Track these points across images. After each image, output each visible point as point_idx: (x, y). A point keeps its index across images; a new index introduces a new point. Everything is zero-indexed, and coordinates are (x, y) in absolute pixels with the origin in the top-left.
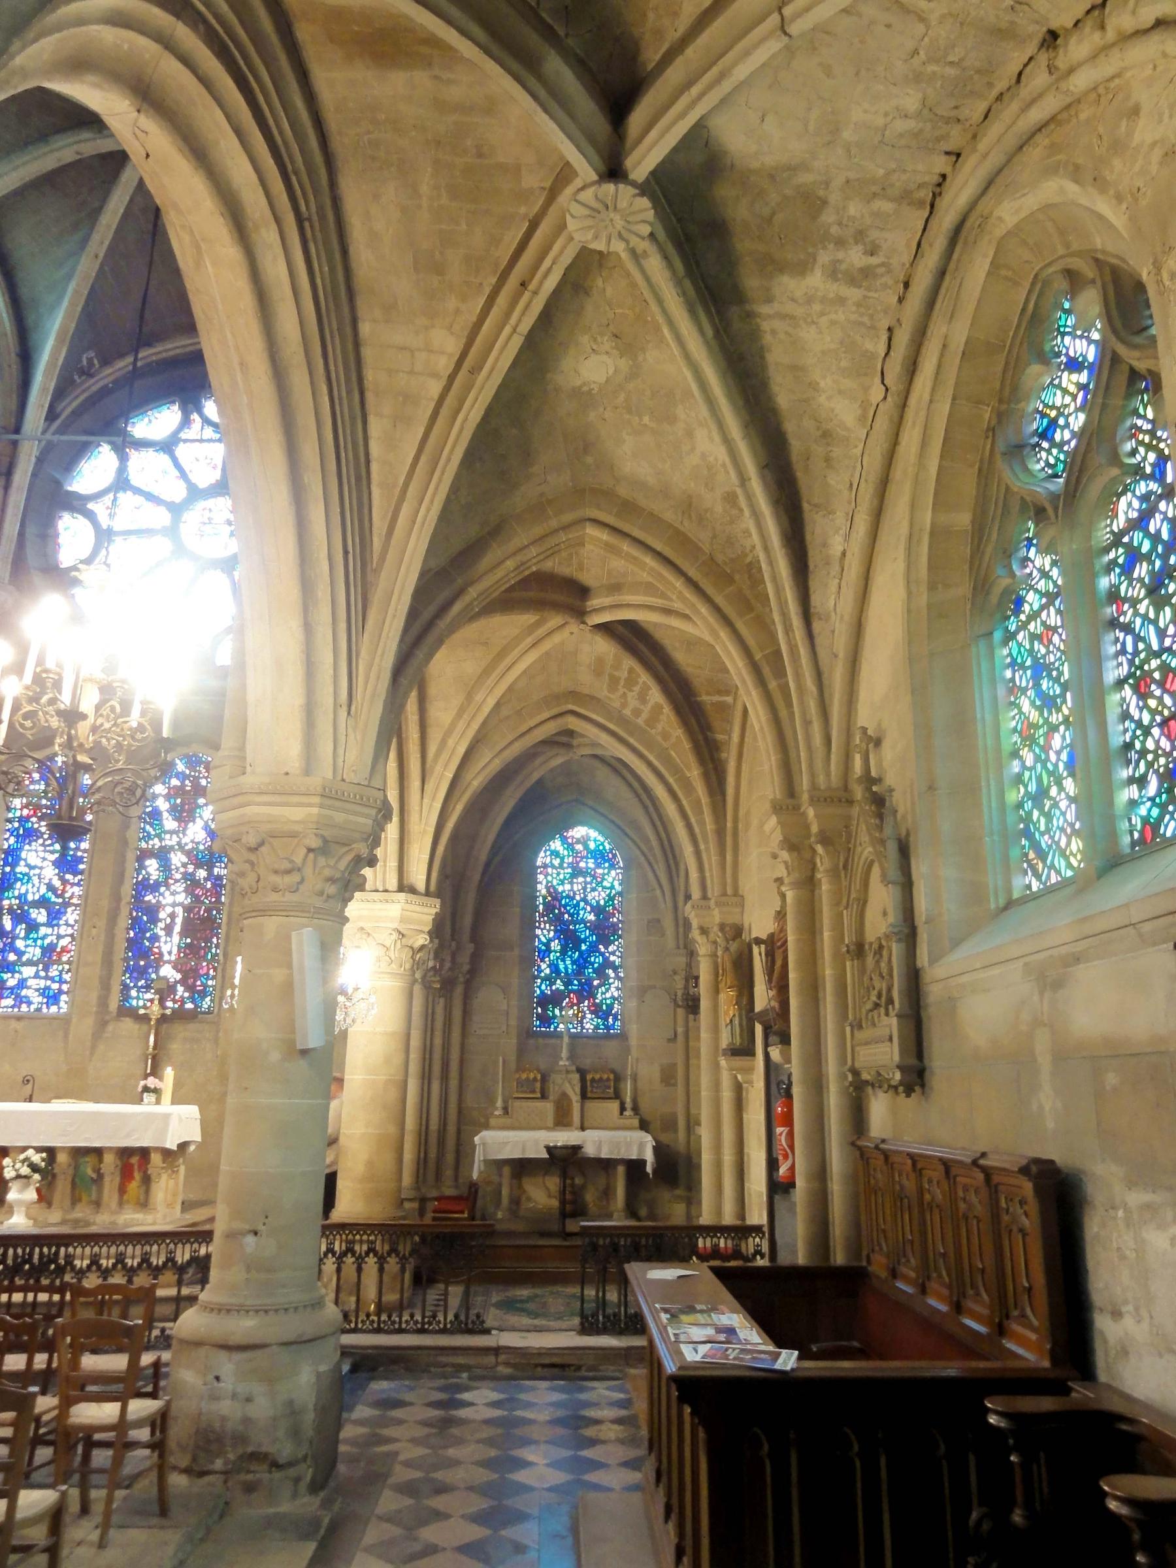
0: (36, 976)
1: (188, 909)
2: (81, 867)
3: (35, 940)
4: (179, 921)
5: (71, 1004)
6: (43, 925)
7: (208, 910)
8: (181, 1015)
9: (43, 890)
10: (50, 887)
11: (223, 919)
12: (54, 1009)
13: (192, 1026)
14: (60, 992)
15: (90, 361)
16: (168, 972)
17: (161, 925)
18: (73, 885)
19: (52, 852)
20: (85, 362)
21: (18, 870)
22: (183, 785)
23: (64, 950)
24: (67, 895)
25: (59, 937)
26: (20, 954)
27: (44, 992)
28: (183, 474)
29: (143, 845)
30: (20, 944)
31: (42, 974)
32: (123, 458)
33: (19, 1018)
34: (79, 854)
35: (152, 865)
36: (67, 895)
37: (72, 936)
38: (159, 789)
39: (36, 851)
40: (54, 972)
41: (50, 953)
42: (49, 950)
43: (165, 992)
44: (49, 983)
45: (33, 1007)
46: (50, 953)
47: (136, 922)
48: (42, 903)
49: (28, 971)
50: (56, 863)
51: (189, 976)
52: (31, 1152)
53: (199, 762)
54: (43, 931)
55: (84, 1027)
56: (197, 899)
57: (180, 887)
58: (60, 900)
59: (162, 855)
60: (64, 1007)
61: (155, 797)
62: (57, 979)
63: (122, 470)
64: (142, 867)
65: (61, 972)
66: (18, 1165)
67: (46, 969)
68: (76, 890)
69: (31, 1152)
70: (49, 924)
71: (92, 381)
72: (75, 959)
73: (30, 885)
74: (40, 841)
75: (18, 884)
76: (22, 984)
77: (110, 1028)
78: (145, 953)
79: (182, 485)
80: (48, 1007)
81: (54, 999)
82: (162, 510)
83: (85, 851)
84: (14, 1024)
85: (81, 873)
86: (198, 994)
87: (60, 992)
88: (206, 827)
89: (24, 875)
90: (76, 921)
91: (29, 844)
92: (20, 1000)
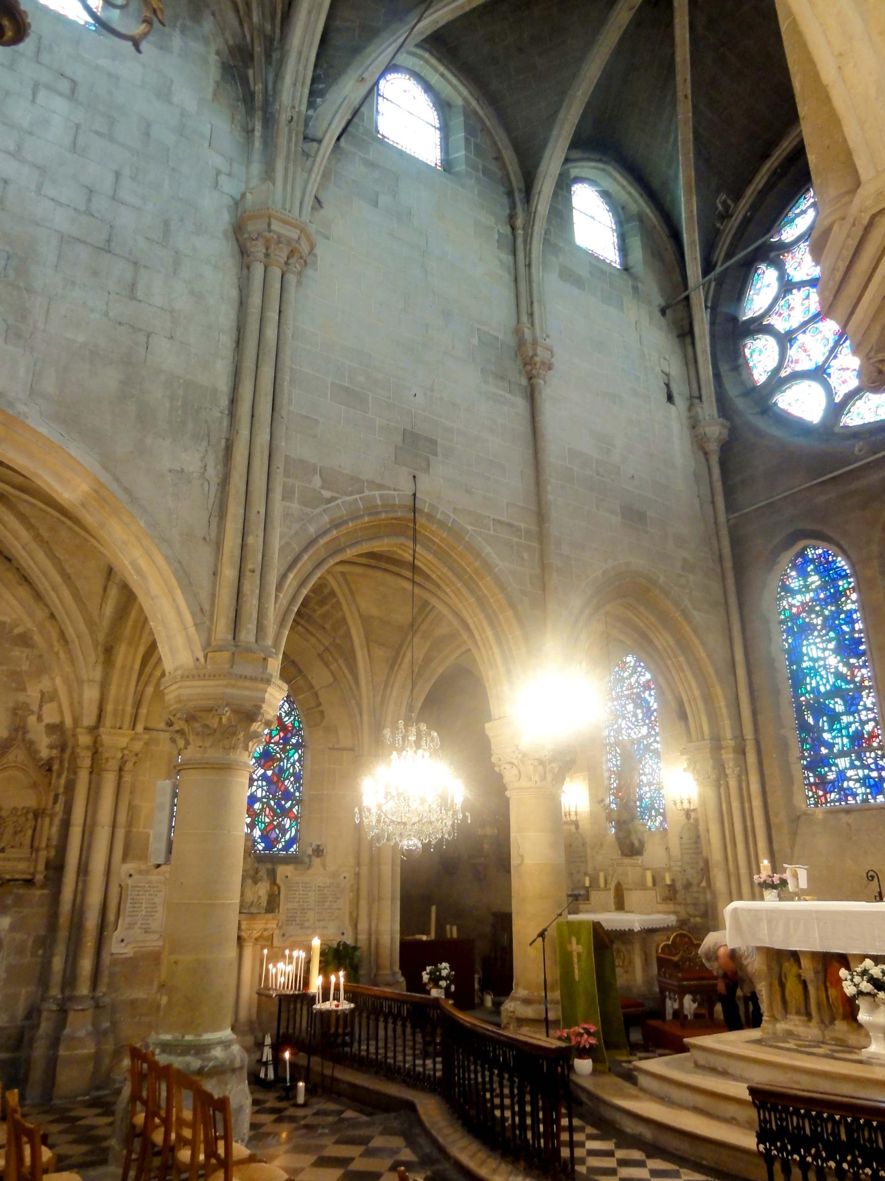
0: (853, 767)
2: (862, 647)
3: (840, 731)
6: (843, 714)
9: (832, 679)
10: (838, 675)
15: (724, 203)
18: (860, 668)
19: (830, 641)
20: (720, 207)
21: (804, 665)
23: (872, 736)
24: (857, 679)
25: (863, 723)
26: (830, 746)
27: (864, 781)
30: (826, 736)
31: (857, 763)
33: (848, 811)
34: (856, 635)
36: (857, 679)
37: (874, 719)
39: (815, 644)
41: (857, 738)
42: (857, 738)
44: (866, 772)
45: (859, 798)
48: (836, 692)
49: (843, 763)
50: (837, 651)
52: (868, 963)
54: (845, 719)
58: (852, 686)
62: (873, 766)
65: (875, 759)
66: (857, 979)
67: (859, 758)
68: (864, 671)
69: (868, 963)
70: (848, 712)
71: (734, 218)
73: (818, 678)
74: (816, 633)
75: (808, 680)
76: (842, 776)
80: (875, 798)
83: (860, 631)
84: (844, 818)
85: (863, 653)
89: (811, 668)
90: (873, 703)
91: (808, 640)
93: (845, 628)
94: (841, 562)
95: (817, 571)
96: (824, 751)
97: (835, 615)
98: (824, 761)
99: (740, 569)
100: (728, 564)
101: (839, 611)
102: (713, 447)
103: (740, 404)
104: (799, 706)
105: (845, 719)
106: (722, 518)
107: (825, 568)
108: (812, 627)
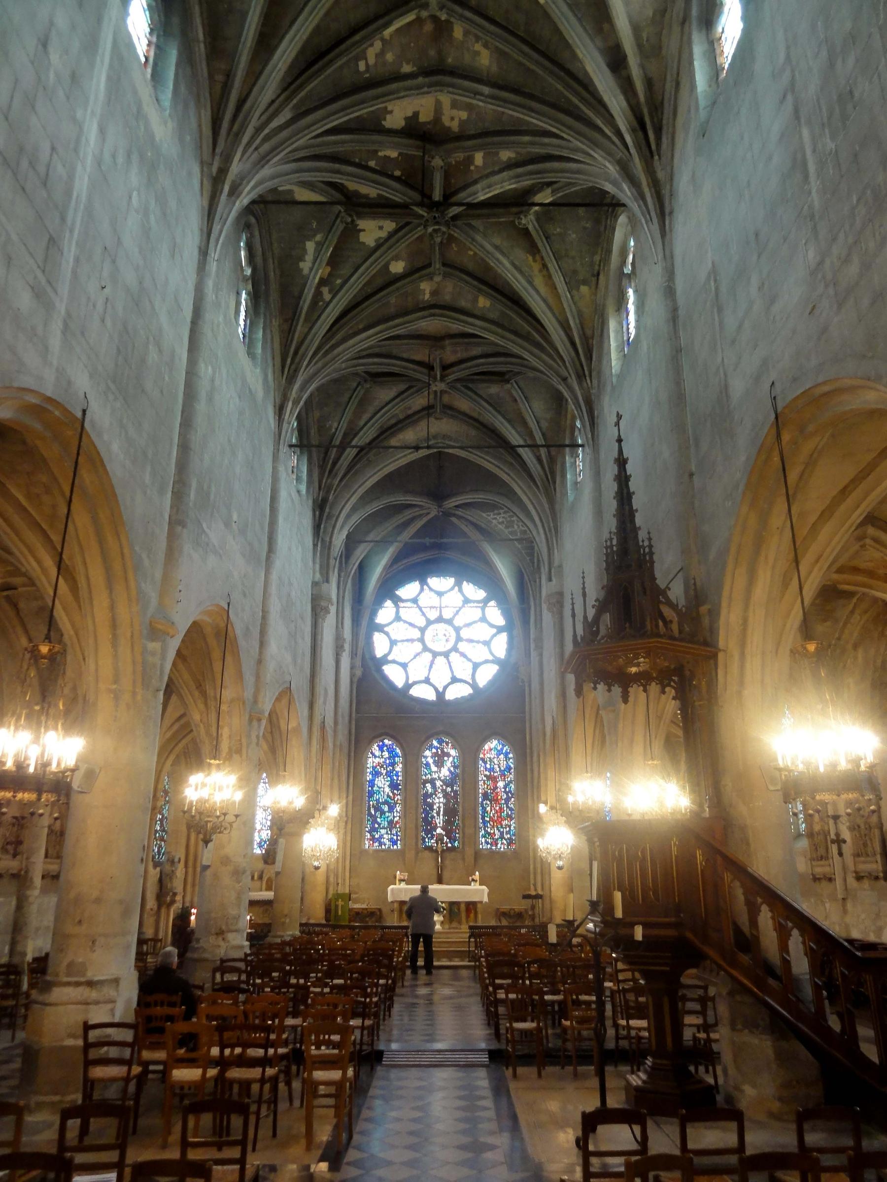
0: (387, 833)
1: (444, 804)
4: (442, 809)
5: (404, 845)
7: (454, 805)
10: (388, 796)
11: (460, 809)
12: (395, 847)
13: (453, 854)
14: (397, 840)
16: (439, 831)
23: (397, 822)
25: (394, 817)
26: (379, 824)
27: (391, 840)
28: (424, 614)
30: (379, 820)
32: (397, 607)
33: (383, 851)
35: (429, 786)
38: (428, 753)
40: (394, 832)
41: (391, 823)
42: (391, 823)
43: (440, 839)
46: (391, 824)
47: (425, 810)
48: (386, 803)
49: (383, 831)
50: (389, 786)
53: (443, 741)
54: (387, 814)
55: (410, 855)
56: (448, 801)
57: (441, 795)
59: (432, 782)
60: (399, 847)
61: (426, 757)
63: (397, 612)
64: (425, 787)
76: (381, 837)
78: (430, 823)
79: (423, 619)
81: (394, 843)
82: (417, 630)
84: (383, 854)
86: (452, 839)
87: (397, 840)
88: (449, 770)
92: (381, 844)
93: (395, 778)
94: (398, 751)
95: (388, 750)
96: (376, 826)
97: (391, 771)
98: (376, 830)
100: (353, 738)
101: (394, 770)
102: (355, 680)
104: (369, 805)
105: (387, 814)
106: (354, 715)
107: (391, 750)
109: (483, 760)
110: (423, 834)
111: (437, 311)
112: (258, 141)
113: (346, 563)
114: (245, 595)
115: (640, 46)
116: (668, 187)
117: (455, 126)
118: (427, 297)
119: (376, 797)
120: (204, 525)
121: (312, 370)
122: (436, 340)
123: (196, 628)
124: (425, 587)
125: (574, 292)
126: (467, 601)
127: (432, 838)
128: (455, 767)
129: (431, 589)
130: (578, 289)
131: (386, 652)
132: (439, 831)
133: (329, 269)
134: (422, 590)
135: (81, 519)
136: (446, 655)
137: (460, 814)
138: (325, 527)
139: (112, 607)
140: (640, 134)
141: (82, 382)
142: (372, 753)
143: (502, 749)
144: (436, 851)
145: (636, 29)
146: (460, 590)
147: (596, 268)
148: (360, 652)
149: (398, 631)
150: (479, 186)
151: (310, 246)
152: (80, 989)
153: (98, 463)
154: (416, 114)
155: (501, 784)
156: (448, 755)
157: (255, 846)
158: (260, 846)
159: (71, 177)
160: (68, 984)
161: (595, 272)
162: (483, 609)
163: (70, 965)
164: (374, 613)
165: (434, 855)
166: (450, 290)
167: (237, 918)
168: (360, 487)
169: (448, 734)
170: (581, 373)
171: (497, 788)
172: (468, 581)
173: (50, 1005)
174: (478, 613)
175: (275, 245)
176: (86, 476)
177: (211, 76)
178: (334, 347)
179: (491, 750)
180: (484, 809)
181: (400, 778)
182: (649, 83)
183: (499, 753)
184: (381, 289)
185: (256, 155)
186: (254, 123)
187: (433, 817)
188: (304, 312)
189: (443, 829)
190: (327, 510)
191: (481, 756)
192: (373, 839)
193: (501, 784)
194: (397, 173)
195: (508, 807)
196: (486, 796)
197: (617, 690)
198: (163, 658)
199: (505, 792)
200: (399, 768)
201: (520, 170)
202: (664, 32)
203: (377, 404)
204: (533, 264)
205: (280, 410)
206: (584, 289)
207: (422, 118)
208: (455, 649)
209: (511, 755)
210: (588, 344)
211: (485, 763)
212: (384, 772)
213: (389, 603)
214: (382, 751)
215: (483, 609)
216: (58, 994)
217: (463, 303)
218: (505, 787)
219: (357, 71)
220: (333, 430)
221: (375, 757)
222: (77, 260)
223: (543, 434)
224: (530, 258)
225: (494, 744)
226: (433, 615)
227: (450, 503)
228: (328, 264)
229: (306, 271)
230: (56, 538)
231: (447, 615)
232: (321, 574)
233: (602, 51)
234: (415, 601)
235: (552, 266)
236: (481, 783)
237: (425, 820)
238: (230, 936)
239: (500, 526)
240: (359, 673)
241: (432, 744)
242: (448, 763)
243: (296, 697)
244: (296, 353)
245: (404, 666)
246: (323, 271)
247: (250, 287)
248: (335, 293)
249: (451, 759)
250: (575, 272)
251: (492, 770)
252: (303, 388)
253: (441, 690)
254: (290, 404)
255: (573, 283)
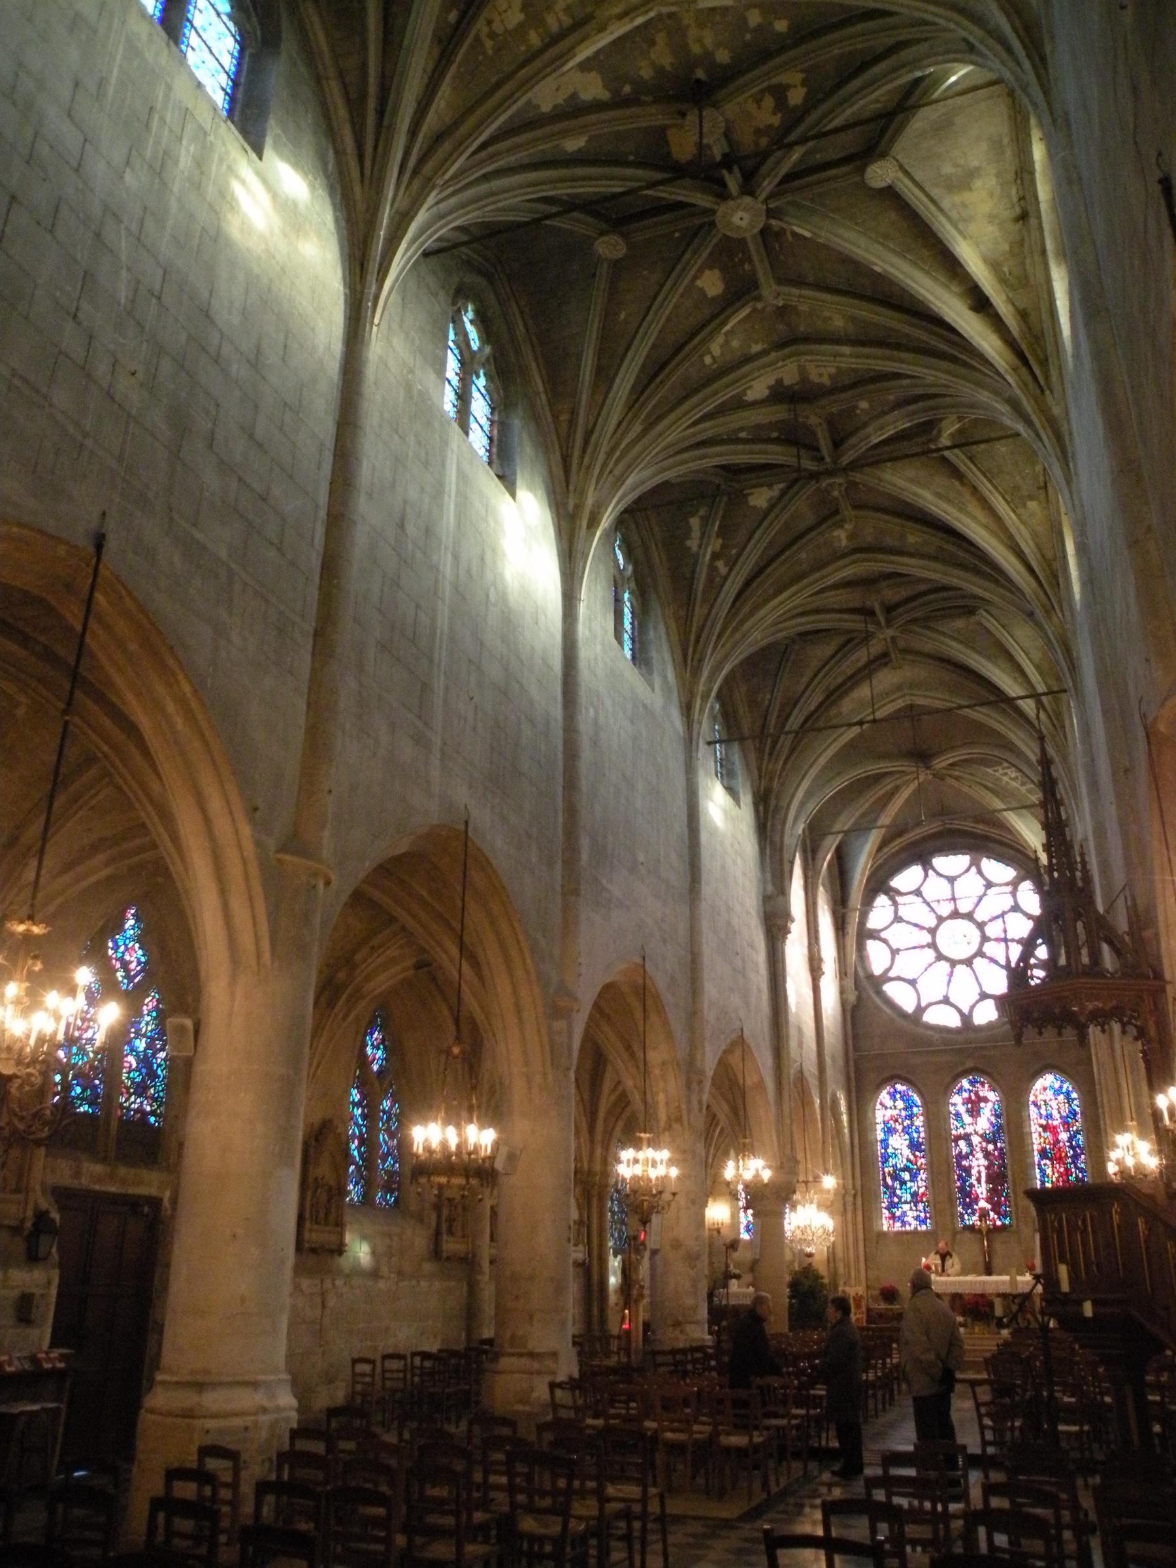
1: (987, 1168)
8: (996, 1229)
9: (905, 1161)
10: (909, 1160)
11: (1009, 1173)
14: (926, 1218)
16: (983, 1204)
17: (974, 1178)
22: (970, 1097)
23: (923, 1194)
27: (917, 1218)
28: (933, 910)
29: (954, 1132)
33: (907, 1233)
35: (962, 1143)
40: (921, 1206)
41: (914, 1195)
42: (914, 1195)
43: (984, 1215)
47: (960, 1176)
49: (906, 1207)
51: (996, 1207)
54: (909, 1184)
57: (980, 1155)
61: (955, 1105)
63: (896, 912)
64: (957, 1145)
67: (916, 1206)
70: (911, 1181)
72: (931, 1199)
76: (904, 1214)
77: (958, 1236)
78: (969, 1194)
84: (909, 1237)
92: (904, 1223)
93: (915, 1135)
94: (916, 1098)
95: (902, 1098)
96: (896, 1200)
97: (909, 1127)
99: (859, 1089)
100: (854, 1084)
101: (912, 1124)
102: (849, 1008)
103: (865, 983)
104: (884, 1174)
105: (909, 1184)
108: (896, 1131)
109: (1035, 1104)
110: (960, 1209)
111: (864, 556)
112: (610, 466)
113: (814, 859)
114: (664, 941)
115: (1002, 280)
116: (1066, 425)
117: (826, 380)
118: (844, 542)
119: (892, 1161)
120: (604, 882)
121: (719, 655)
122: (867, 582)
123: (609, 988)
124: (931, 872)
125: (1021, 511)
126: (989, 885)
127: (974, 1214)
128: (997, 1116)
129: (939, 874)
130: (1025, 506)
131: (887, 965)
132: (983, 1204)
133: (720, 541)
134: (926, 876)
135: (476, 917)
136: (968, 962)
137: (1010, 1177)
138: (773, 825)
139: (515, 993)
140: (1024, 371)
141: (462, 795)
142: (881, 1104)
143: (1061, 1087)
144: (980, 1231)
145: (994, 266)
146: (980, 872)
147: (1042, 478)
148: (851, 971)
149: (899, 935)
150: (870, 429)
151: (695, 522)
152: (523, 1360)
153: (484, 864)
154: (779, 382)
155: (1063, 1136)
156: (986, 1100)
157: (742, 1230)
158: (748, 1230)
159: (433, 620)
160: (513, 1355)
161: (1042, 484)
162: (1014, 894)
163: (513, 1337)
164: (864, 917)
165: (978, 1236)
166: (872, 526)
167: (695, 1308)
168: (811, 766)
169: (983, 1072)
170: (1049, 607)
171: (1058, 1141)
172: (988, 857)
173: (496, 1372)
174: (1009, 902)
175: (656, 529)
176: (476, 876)
177: (555, 417)
178: (742, 622)
179: (1045, 1089)
180: (1043, 1172)
181: (922, 1135)
182: (1023, 315)
183: (1058, 1092)
184: (782, 551)
185: (611, 478)
186: (605, 448)
187: (972, 1186)
188: (699, 594)
189: (988, 1200)
190: (773, 802)
191: (1032, 1098)
192: (893, 1217)
193: (1063, 1136)
194: (775, 435)
195: (1076, 1168)
196: (1043, 1154)
197: (1070, 1034)
198: (570, 1037)
199: (1071, 1147)
200: (919, 1122)
201: (912, 407)
202: (1028, 261)
203: (814, 664)
204: (961, 488)
205: (687, 710)
206: (1033, 505)
207: (787, 382)
208: (980, 953)
209: (1074, 1095)
210: (1050, 566)
211: (1039, 1107)
212: (900, 1128)
213: (882, 900)
214: (895, 1100)
215: (1014, 894)
216: (505, 1362)
217: (889, 541)
218: (1070, 1139)
219: (704, 366)
220: (767, 703)
221: (886, 1108)
222: (447, 688)
223: (1037, 667)
224: (957, 483)
225: (1048, 1080)
226: (945, 909)
227: (940, 763)
228: (718, 536)
229: (695, 548)
230: (458, 927)
231: (964, 908)
232: (774, 885)
233: (960, 296)
234: (918, 892)
235: (986, 487)
236: (1035, 1136)
237: (962, 1189)
238: (689, 1328)
239: (1014, 784)
240: (852, 997)
241: (962, 1087)
242: (987, 1110)
243: (752, 1044)
244: (697, 641)
245: (912, 983)
246: (716, 544)
247: (633, 584)
248: (732, 564)
249: (990, 1105)
250: (1016, 488)
251: (1049, 1116)
252: (712, 678)
253: (966, 1011)
254: (699, 701)
255: (1017, 500)
